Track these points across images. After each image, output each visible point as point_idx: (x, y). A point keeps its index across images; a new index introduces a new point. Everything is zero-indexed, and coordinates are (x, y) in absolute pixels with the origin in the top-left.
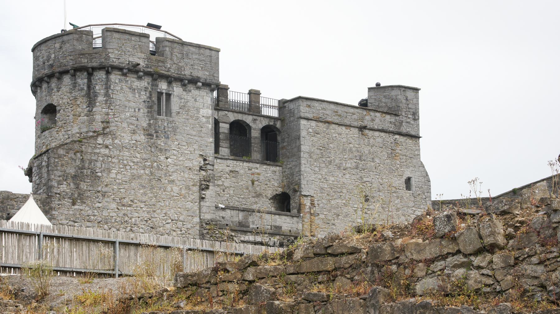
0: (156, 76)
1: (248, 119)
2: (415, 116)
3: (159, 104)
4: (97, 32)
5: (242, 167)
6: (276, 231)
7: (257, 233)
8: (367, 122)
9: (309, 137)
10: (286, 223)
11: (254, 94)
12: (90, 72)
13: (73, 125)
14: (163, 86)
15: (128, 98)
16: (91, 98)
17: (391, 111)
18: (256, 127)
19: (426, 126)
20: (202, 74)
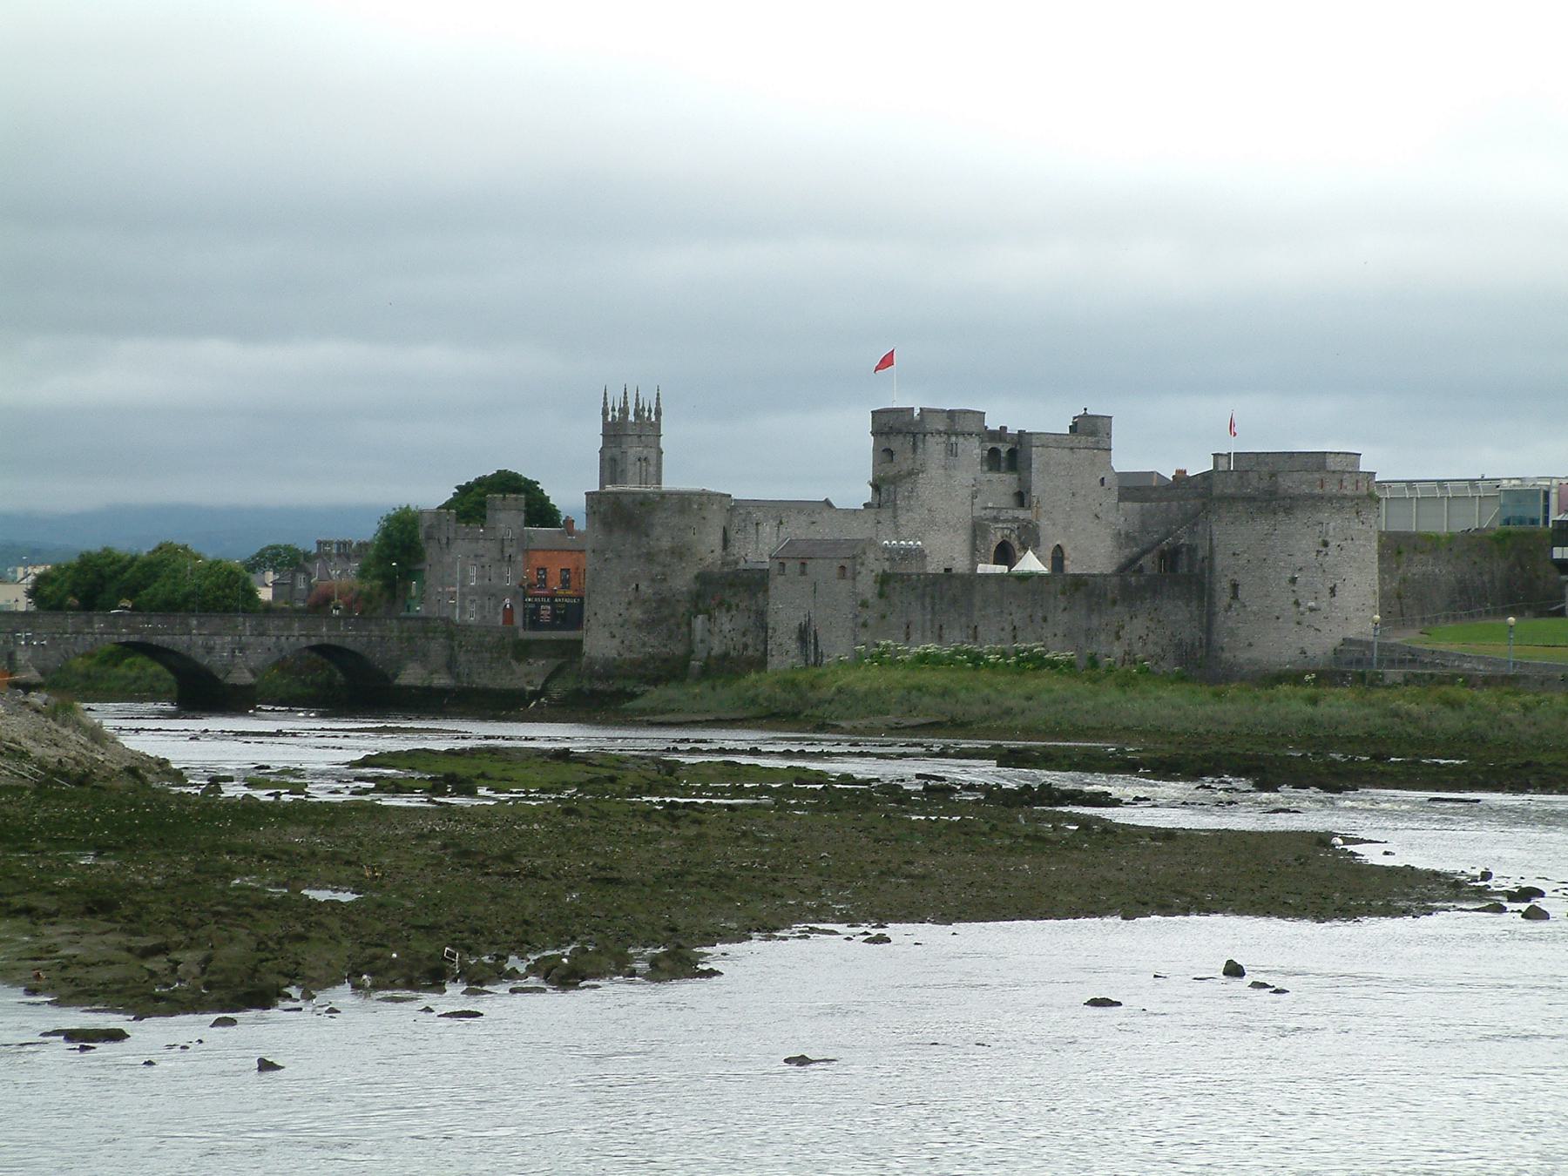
0: (948, 434)
1: (999, 446)
2: (1109, 435)
3: (952, 451)
4: (917, 411)
5: (995, 476)
6: (1016, 519)
7: (1004, 521)
8: (1075, 444)
9: (1037, 456)
10: (1021, 514)
11: (1003, 429)
12: (914, 435)
13: (903, 462)
14: (953, 439)
15: (934, 448)
16: (915, 448)
17: (1091, 431)
18: (1004, 449)
19: (1115, 442)
20: (975, 430)
